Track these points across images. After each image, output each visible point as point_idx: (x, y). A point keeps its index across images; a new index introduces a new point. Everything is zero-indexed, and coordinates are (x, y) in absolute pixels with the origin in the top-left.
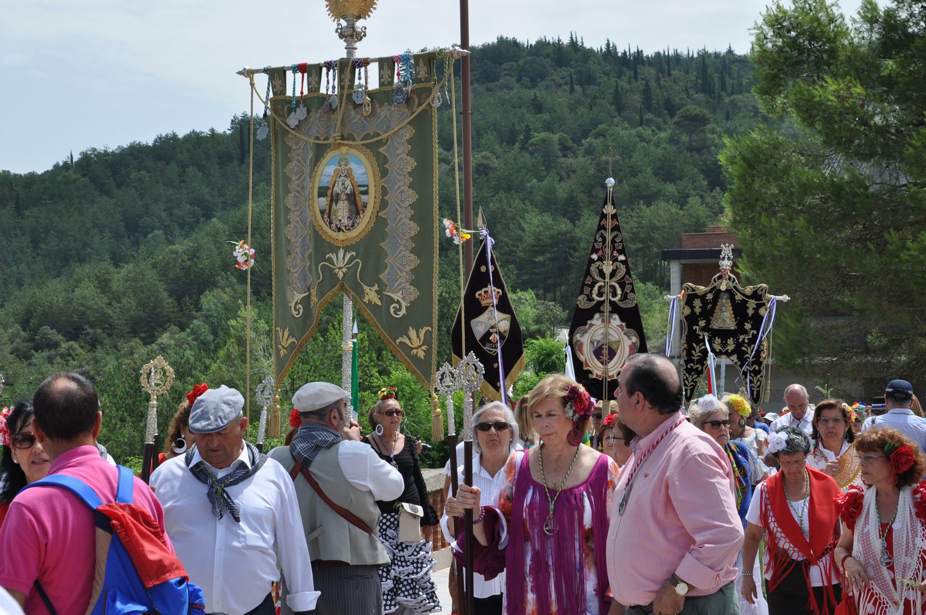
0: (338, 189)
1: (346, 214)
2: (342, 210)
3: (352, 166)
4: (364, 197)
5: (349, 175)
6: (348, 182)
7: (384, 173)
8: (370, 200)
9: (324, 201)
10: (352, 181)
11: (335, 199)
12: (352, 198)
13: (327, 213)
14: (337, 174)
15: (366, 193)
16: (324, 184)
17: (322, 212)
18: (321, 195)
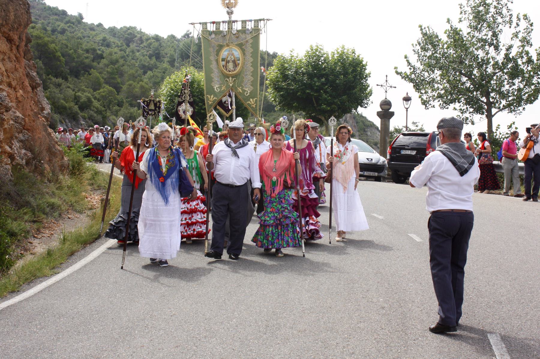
0: (229, 59)
1: (232, 67)
2: (231, 66)
3: (234, 52)
4: (238, 62)
5: (233, 55)
6: (232, 57)
7: (244, 54)
8: (240, 62)
9: (224, 63)
10: (234, 56)
11: (228, 62)
12: (234, 62)
13: (225, 66)
14: (229, 54)
15: (239, 60)
16: (224, 57)
17: (223, 66)
18: (222, 61)
